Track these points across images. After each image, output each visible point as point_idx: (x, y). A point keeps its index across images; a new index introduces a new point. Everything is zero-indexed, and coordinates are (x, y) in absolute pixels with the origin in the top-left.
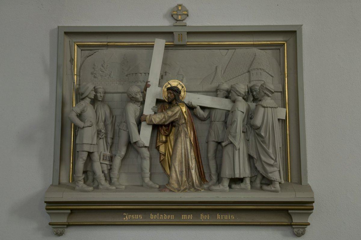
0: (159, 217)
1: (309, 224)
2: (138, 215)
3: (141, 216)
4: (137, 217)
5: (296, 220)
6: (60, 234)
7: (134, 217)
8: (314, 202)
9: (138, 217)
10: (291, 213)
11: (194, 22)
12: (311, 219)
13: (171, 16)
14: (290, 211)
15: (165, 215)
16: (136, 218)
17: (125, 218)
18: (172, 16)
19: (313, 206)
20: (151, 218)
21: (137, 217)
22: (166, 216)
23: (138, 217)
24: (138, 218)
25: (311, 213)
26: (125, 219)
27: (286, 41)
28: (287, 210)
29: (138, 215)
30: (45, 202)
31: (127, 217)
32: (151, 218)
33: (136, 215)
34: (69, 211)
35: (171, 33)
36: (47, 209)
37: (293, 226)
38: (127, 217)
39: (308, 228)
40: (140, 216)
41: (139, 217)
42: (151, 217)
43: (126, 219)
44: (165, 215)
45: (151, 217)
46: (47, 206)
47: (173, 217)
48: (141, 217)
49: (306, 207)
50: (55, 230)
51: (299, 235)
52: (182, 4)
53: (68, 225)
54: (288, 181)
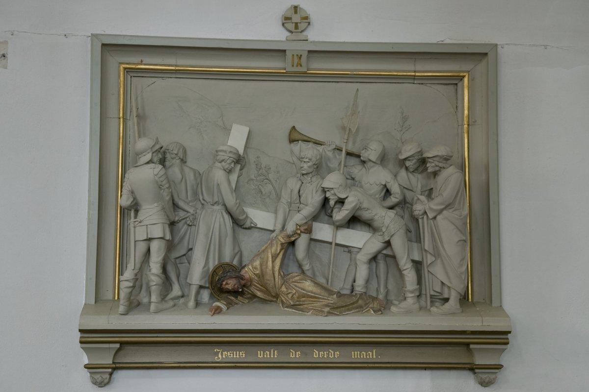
0: (360, 355)
1: (499, 367)
2: (238, 352)
3: (230, 356)
4: (236, 356)
5: (479, 360)
6: (102, 384)
7: (232, 355)
8: (510, 332)
9: (238, 354)
10: (472, 349)
11: (320, 34)
12: (505, 359)
13: (280, 23)
14: (472, 346)
15: (315, 350)
16: (235, 357)
17: (218, 356)
18: (283, 24)
19: (508, 339)
20: (315, 356)
21: (236, 356)
22: (317, 352)
23: (238, 354)
24: (238, 357)
25: (505, 349)
26: (217, 358)
27: (468, 72)
28: (468, 344)
29: (238, 352)
30: (80, 331)
31: (220, 356)
32: (315, 356)
33: (235, 353)
34: (118, 346)
35: (281, 53)
36: (81, 342)
37: (477, 371)
38: (220, 356)
39: (501, 375)
40: (241, 353)
41: (239, 355)
42: (259, 354)
43: (219, 358)
44: (315, 350)
45: (259, 354)
46: (81, 337)
47: (353, 354)
48: (244, 355)
49: (500, 338)
50: (97, 377)
51: (484, 384)
52: (299, 5)
53: (115, 369)
54: (468, 299)
